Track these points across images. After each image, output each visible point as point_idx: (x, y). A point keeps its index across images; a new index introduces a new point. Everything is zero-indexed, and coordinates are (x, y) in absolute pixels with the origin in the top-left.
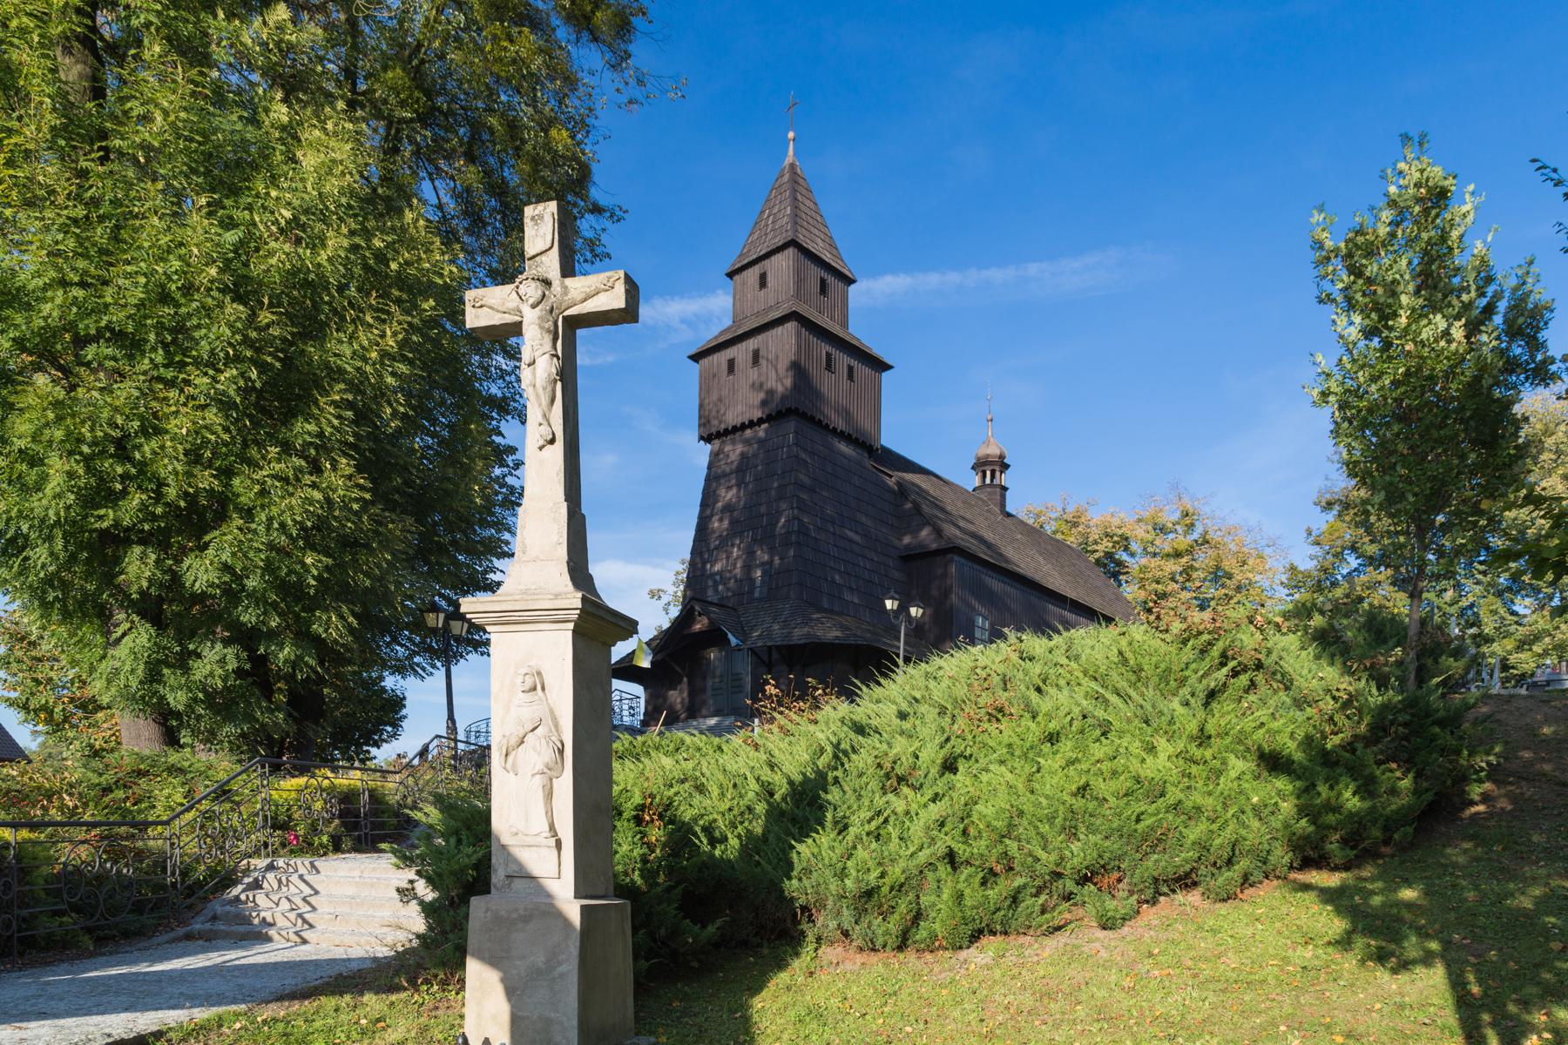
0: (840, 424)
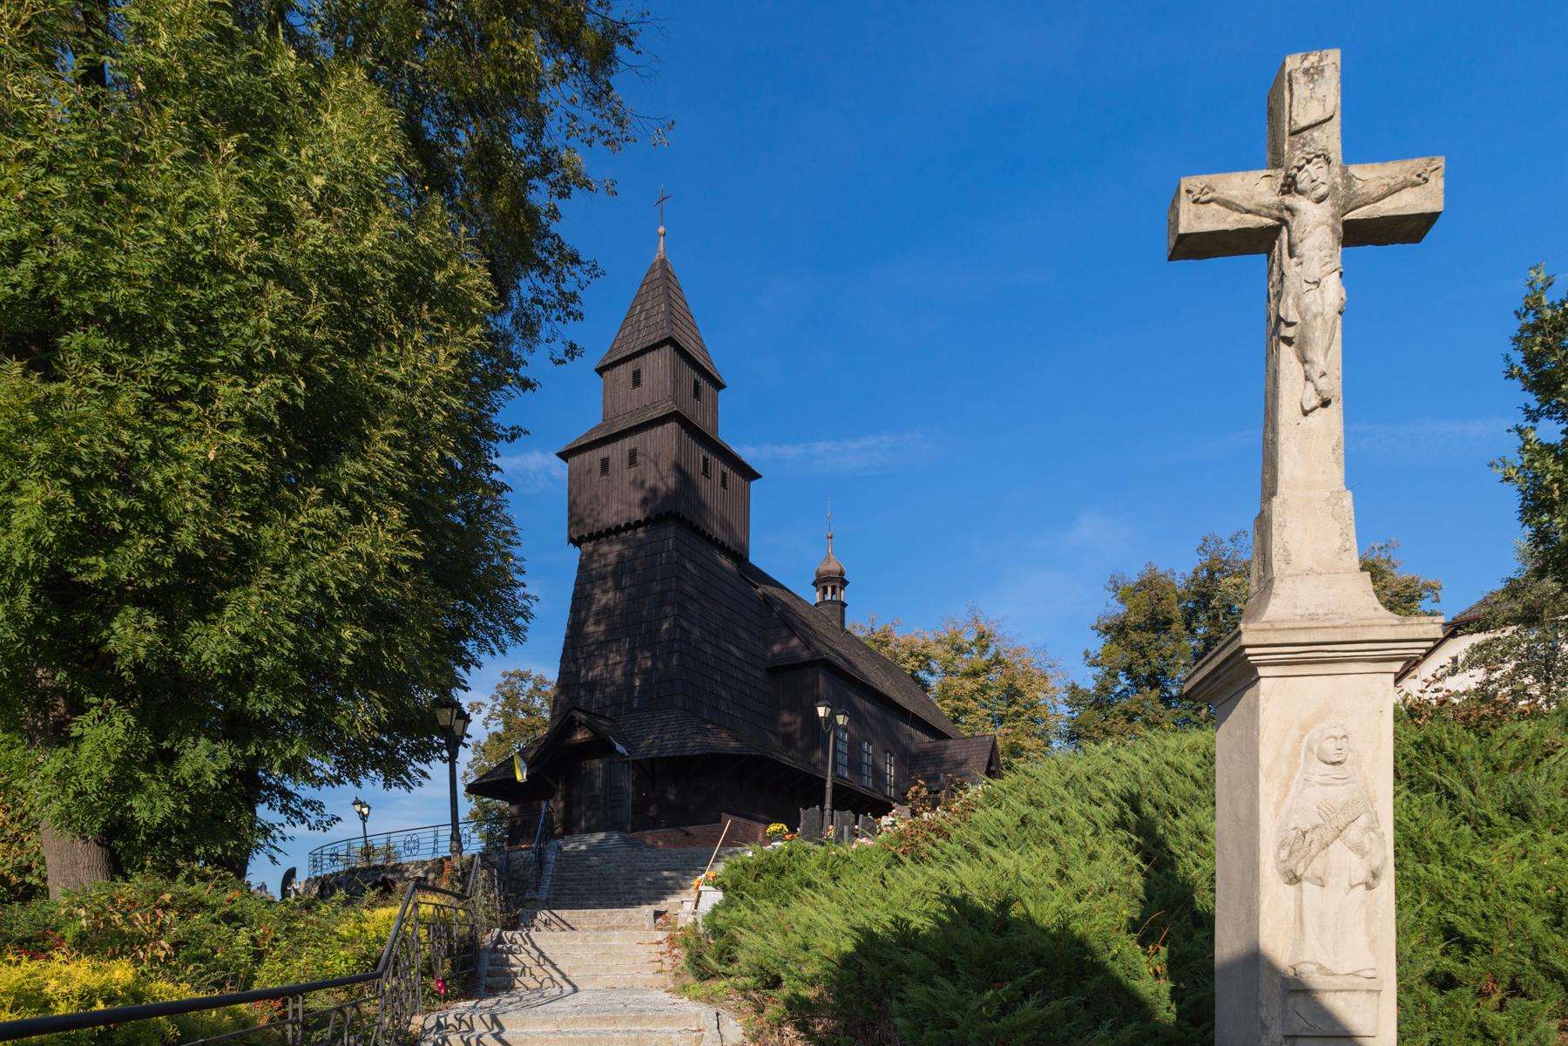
0: (717, 532)
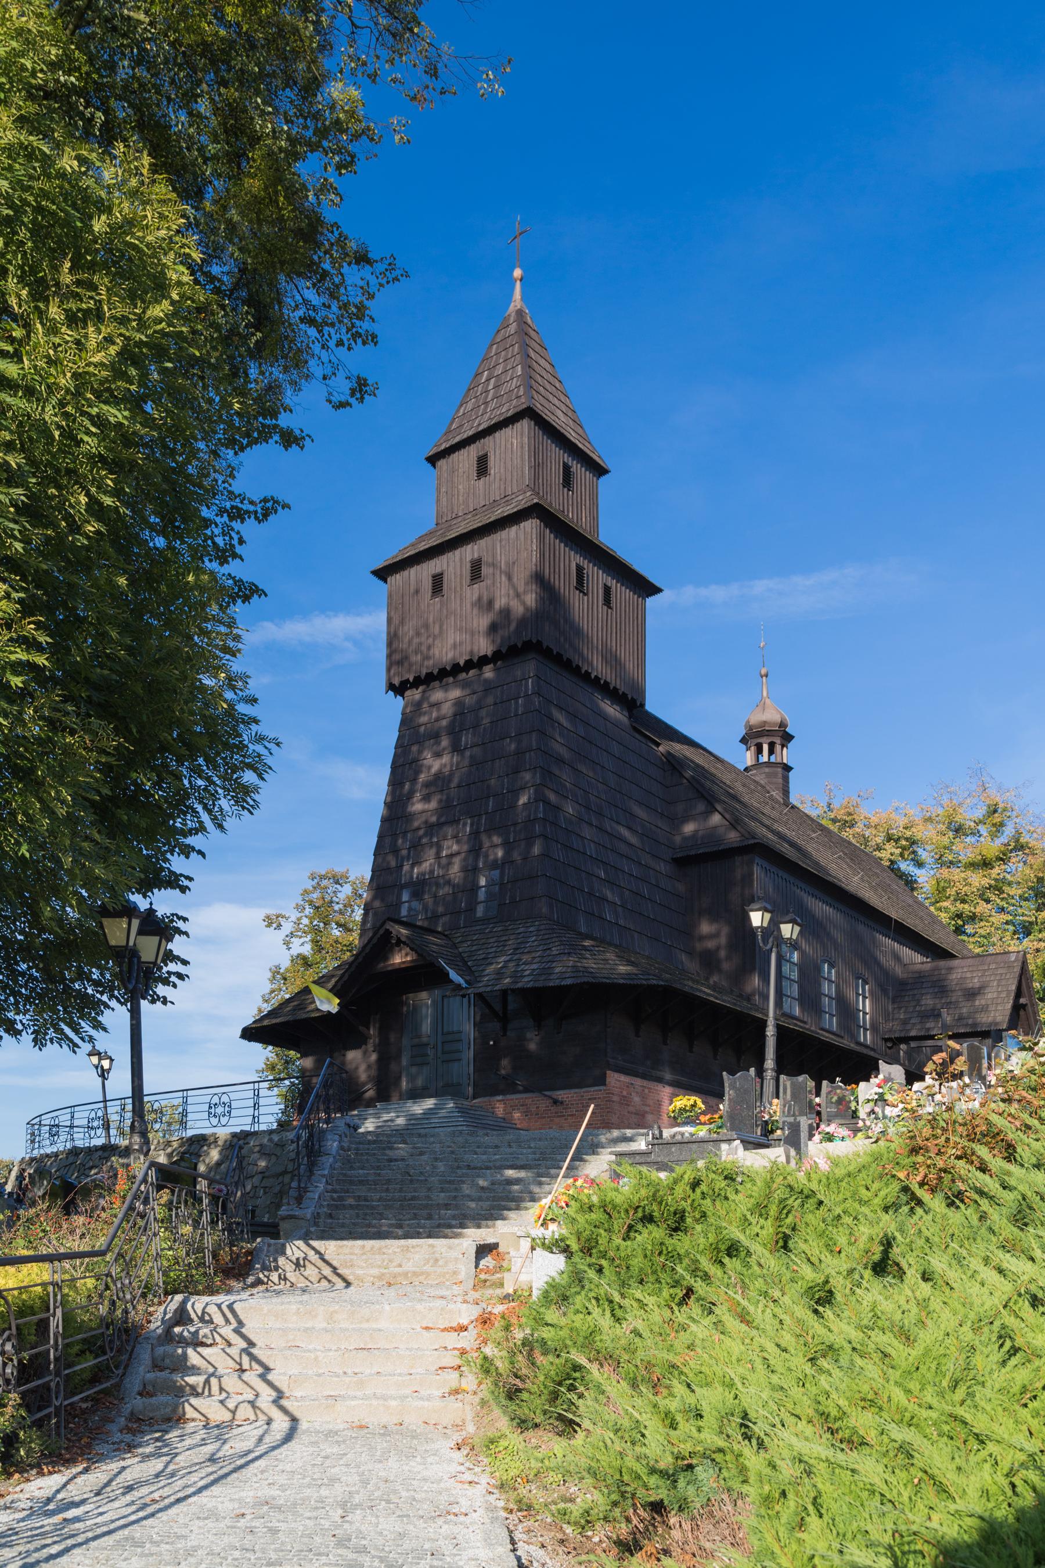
0: (599, 668)
